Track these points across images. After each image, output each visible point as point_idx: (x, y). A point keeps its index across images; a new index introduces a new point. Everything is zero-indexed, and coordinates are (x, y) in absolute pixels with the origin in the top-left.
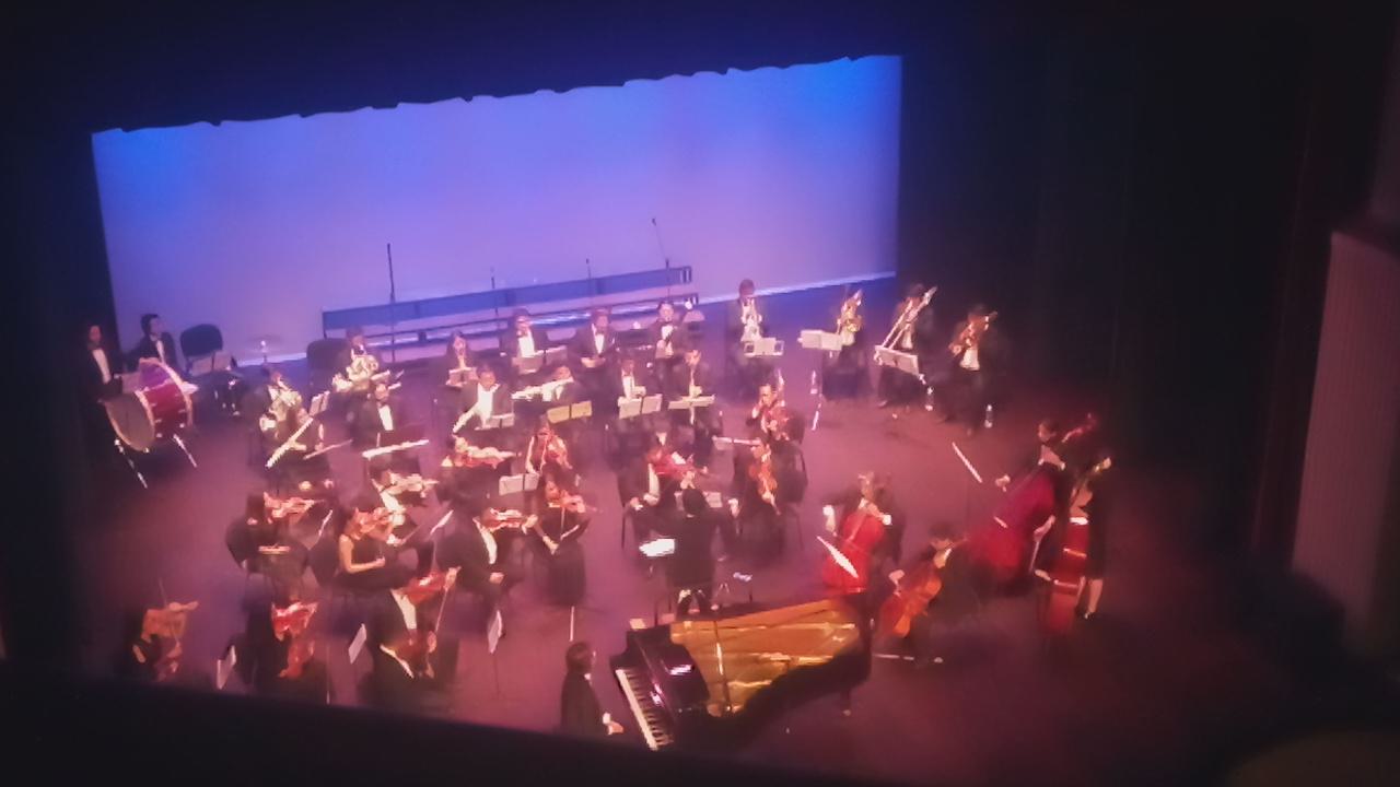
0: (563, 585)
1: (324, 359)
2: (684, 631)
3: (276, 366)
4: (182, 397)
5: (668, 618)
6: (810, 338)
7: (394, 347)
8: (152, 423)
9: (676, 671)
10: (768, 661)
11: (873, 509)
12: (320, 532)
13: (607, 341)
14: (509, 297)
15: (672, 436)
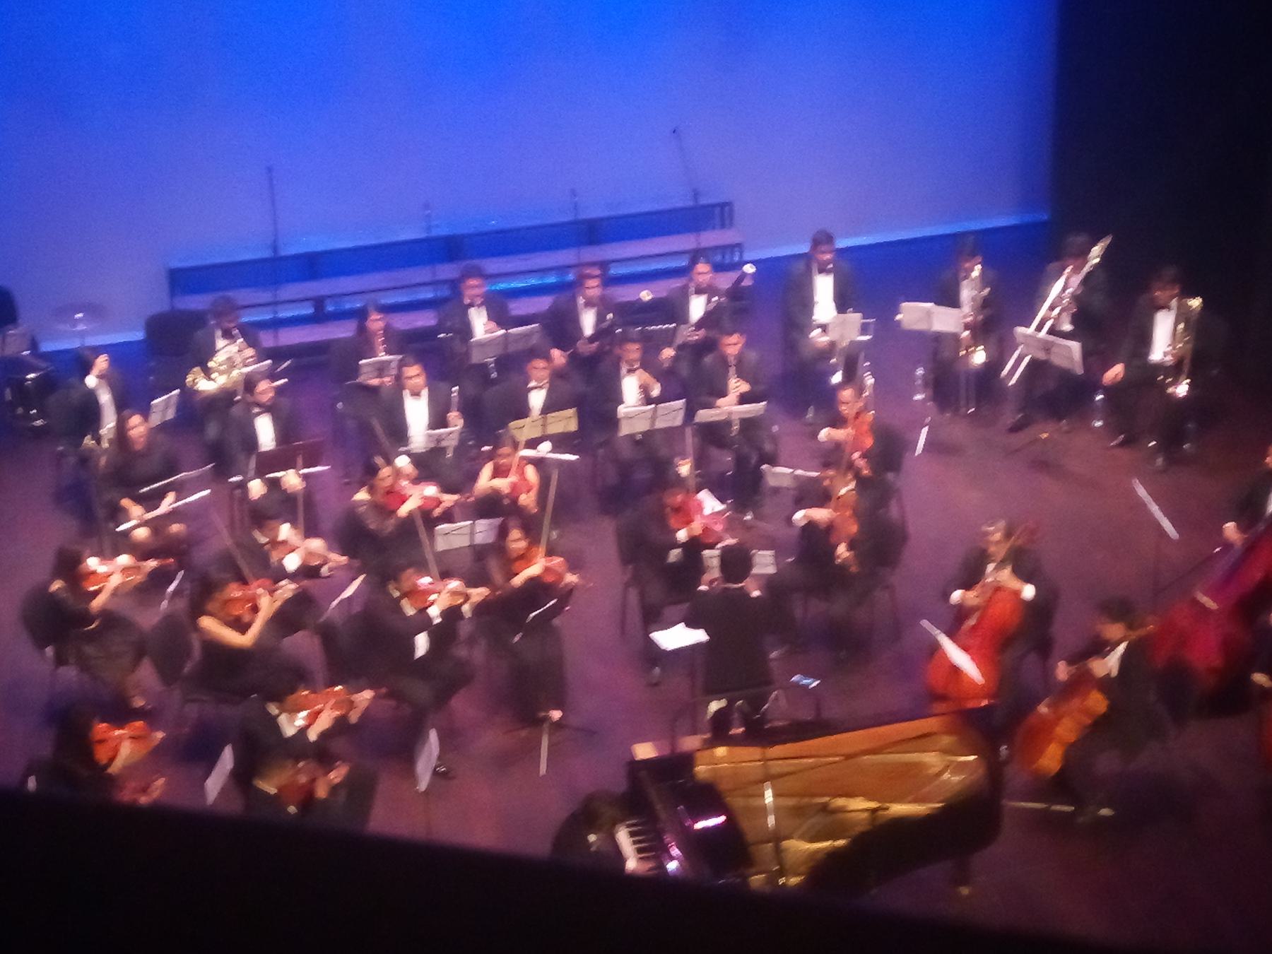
0: (529, 691)
1: (171, 345)
2: (716, 761)
5: (690, 743)
7: (277, 324)
9: (699, 825)
10: (842, 810)
11: (1006, 576)
12: (165, 604)
13: (600, 318)
14: (450, 249)
15: (699, 462)
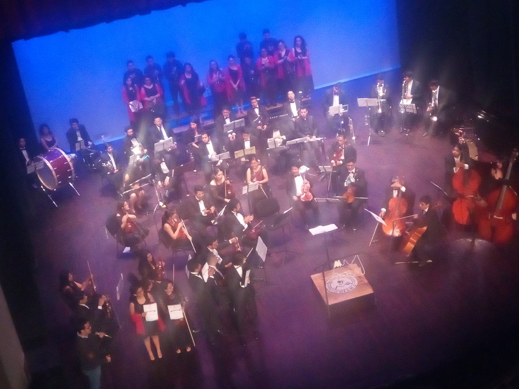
3: (110, 143)
4: (68, 164)
6: (362, 102)
8: (56, 177)
